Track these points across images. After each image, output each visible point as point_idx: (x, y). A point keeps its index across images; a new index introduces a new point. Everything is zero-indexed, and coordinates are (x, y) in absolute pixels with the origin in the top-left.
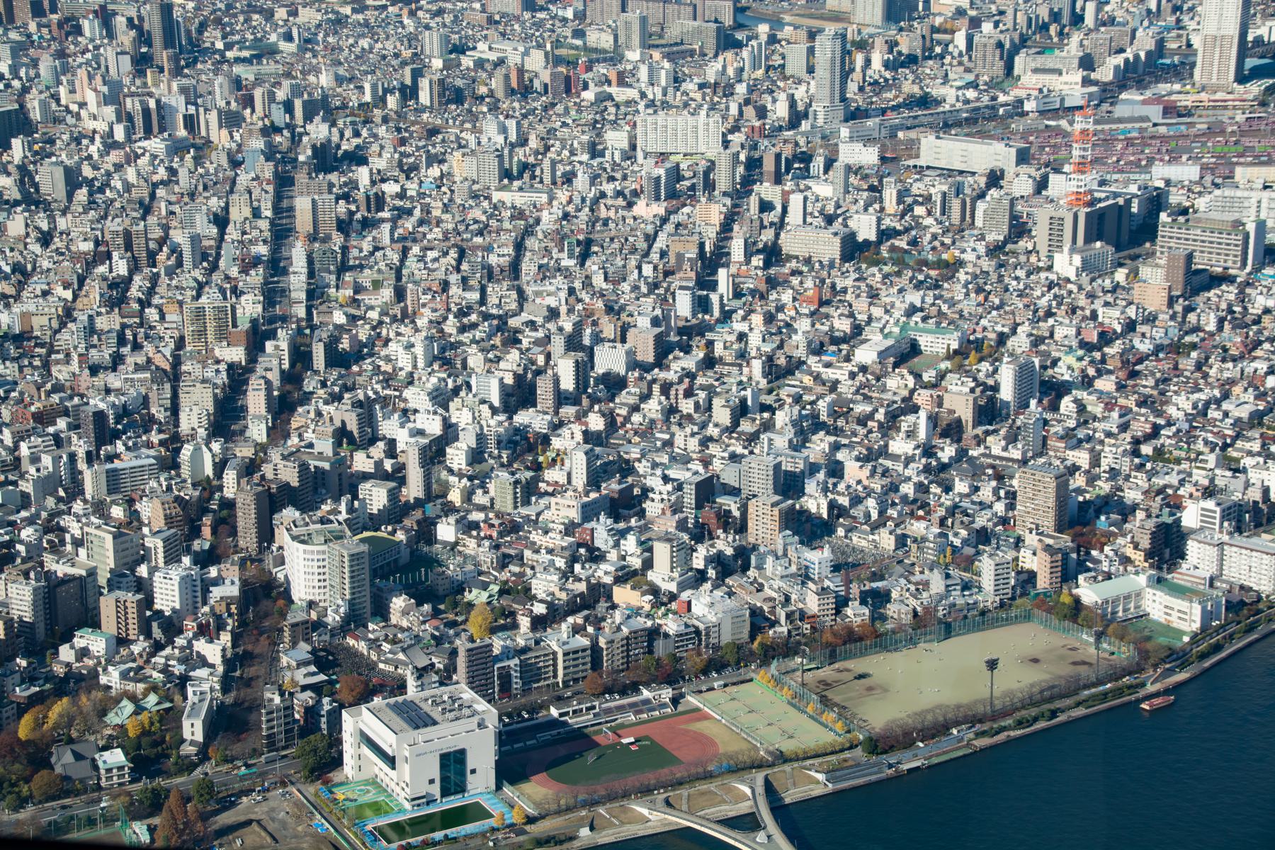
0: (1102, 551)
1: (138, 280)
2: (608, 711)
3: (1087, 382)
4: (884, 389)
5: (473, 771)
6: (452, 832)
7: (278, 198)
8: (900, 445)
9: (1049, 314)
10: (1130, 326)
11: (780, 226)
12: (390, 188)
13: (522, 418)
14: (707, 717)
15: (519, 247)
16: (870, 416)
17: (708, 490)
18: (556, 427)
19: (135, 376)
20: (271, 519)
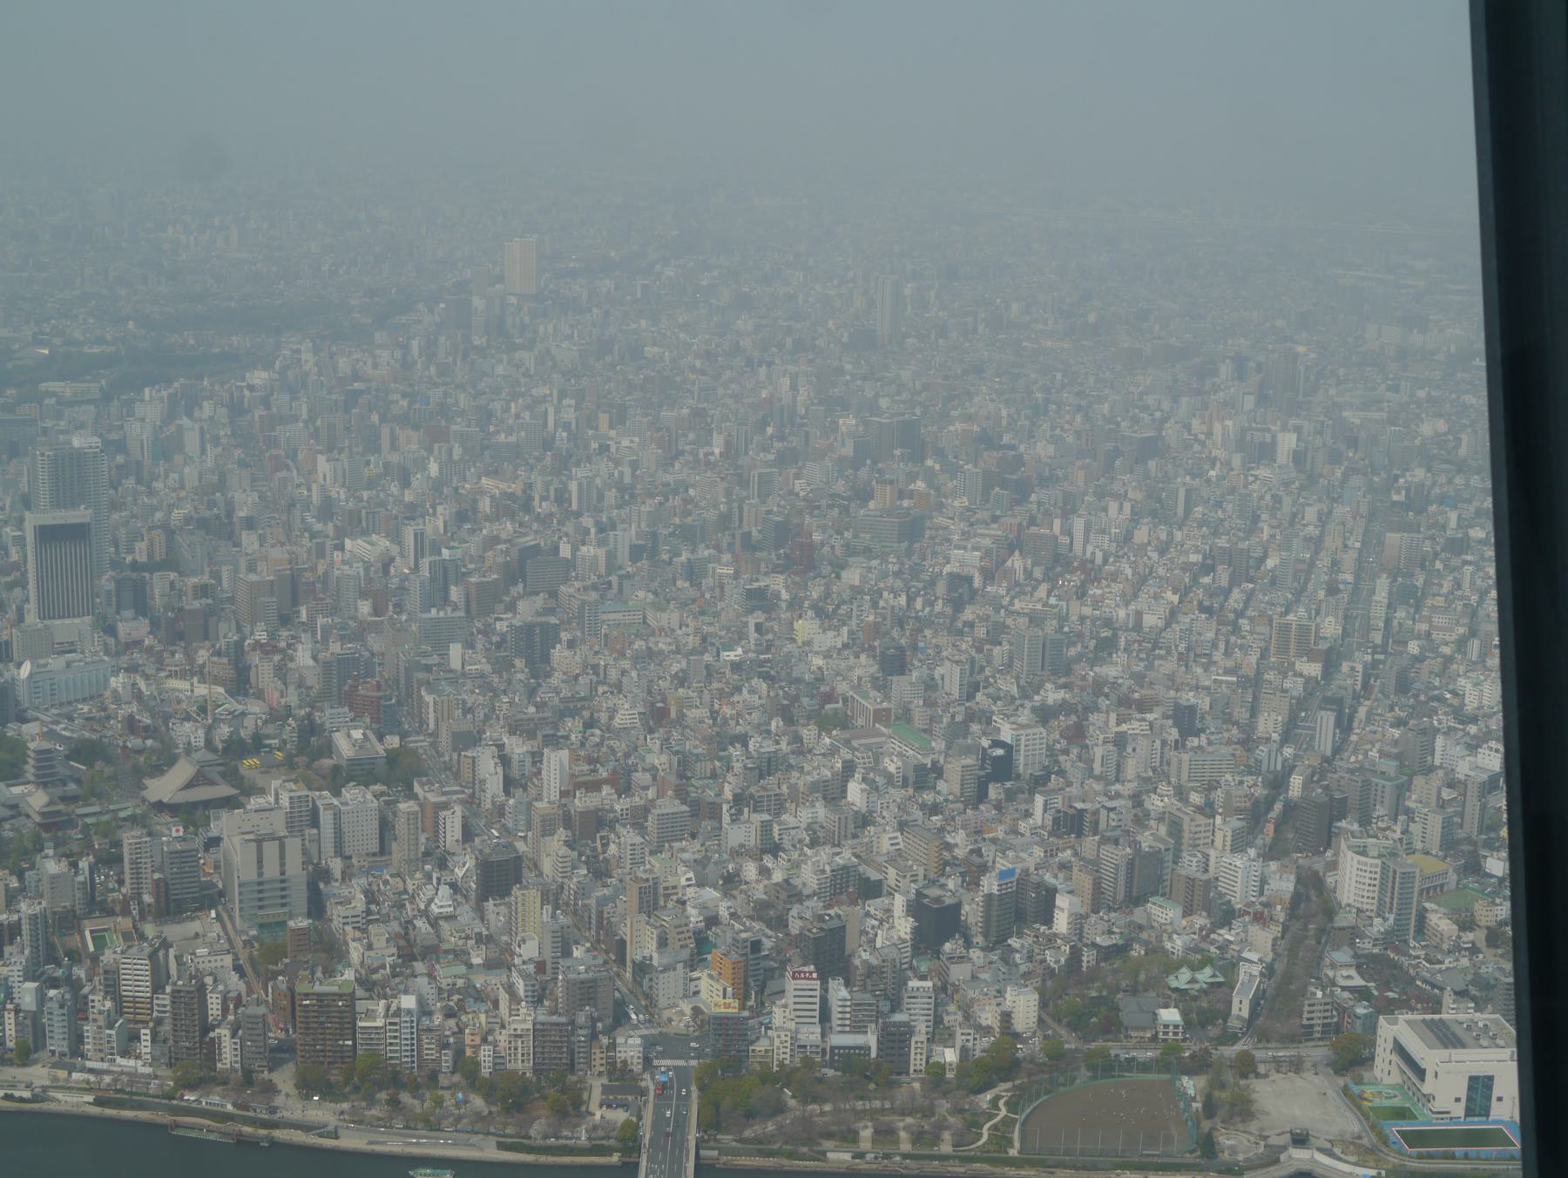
1: (1236, 591)
5: (1500, 1099)
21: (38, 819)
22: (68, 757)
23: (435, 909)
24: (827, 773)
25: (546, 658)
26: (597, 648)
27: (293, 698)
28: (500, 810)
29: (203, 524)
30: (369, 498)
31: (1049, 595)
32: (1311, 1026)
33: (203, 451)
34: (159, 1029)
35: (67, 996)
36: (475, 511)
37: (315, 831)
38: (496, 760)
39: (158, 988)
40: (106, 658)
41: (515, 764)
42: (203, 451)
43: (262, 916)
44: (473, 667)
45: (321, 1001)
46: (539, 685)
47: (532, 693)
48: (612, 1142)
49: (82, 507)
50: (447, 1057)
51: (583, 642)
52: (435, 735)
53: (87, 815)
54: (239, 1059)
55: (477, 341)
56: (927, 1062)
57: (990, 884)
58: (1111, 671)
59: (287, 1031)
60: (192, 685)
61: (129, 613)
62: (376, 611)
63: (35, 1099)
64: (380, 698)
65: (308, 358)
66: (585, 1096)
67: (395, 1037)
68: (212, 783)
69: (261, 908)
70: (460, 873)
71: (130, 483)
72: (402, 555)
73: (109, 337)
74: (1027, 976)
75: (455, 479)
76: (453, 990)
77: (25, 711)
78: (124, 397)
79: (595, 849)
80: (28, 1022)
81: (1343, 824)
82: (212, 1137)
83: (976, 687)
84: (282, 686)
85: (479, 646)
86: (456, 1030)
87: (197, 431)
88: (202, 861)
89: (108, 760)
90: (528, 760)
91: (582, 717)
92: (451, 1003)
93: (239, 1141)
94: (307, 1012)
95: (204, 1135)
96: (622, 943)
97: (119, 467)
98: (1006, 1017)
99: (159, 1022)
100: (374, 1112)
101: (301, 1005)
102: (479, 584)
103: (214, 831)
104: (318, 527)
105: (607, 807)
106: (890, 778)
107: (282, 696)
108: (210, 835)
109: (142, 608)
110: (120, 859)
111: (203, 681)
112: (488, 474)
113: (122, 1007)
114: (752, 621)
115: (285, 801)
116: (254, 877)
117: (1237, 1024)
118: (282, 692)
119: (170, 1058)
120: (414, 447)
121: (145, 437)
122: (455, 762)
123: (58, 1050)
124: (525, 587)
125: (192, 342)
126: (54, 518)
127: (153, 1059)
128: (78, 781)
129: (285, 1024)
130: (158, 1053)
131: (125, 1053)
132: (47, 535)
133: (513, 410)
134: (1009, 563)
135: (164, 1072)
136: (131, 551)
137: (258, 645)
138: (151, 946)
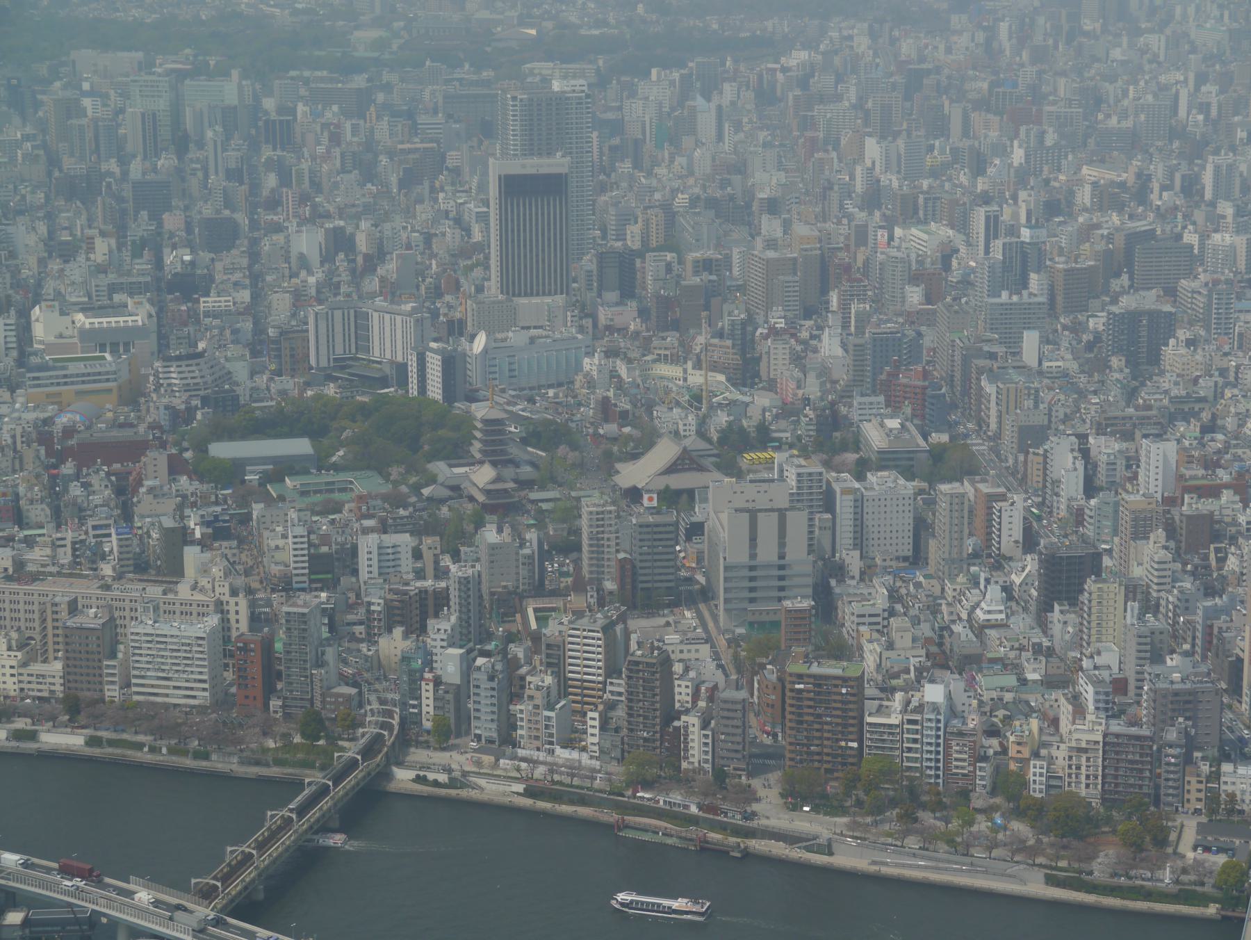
21: (481, 498)
22: (525, 441)
23: (980, 615)
25: (1155, 358)
26: (1227, 348)
27: (812, 388)
28: (1078, 517)
29: (712, 203)
30: (930, 187)
33: (720, 138)
34: (612, 714)
35: (499, 667)
36: (1070, 204)
37: (829, 516)
38: (1076, 454)
39: (612, 671)
40: (580, 336)
41: (1102, 469)
42: (720, 138)
43: (754, 612)
44: (1054, 364)
45: (820, 686)
46: (1143, 384)
47: (1131, 395)
48: (1207, 889)
49: (559, 154)
50: (984, 773)
51: (1207, 341)
52: (998, 436)
53: (542, 501)
54: (710, 757)
55: (1088, 25)
59: (775, 736)
60: (685, 371)
61: (612, 296)
62: (929, 299)
63: (453, 784)
64: (925, 388)
65: (862, 43)
66: (1173, 836)
67: (915, 741)
68: (701, 469)
69: (752, 600)
70: (1017, 579)
71: (625, 166)
72: (968, 244)
73: (612, 21)
75: (1046, 168)
76: (998, 703)
77: (477, 390)
78: (623, 79)
79: (1206, 558)
80: (450, 697)
82: (669, 841)
84: (797, 373)
85: (1065, 344)
86: (999, 749)
87: (713, 113)
88: (682, 555)
89: (574, 447)
90: (1121, 463)
91: (1199, 420)
92: (995, 720)
93: (703, 849)
94: (799, 699)
95: (659, 838)
96: (1240, 661)
97: (613, 149)
99: (611, 706)
100: (887, 827)
101: (792, 690)
102: (1068, 272)
103: (698, 516)
104: (861, 216)
105: (1227, 519)
107: (799, 387)
108: (694, 519)
109: (628, 287)
110: (578, 548)
111: (698, 365)
112: (1090, 163)
113: (566, 686)
116: (744, 559)
118: (799, 381)
119: (623, 751)
120: (994, 134)
121: (647, 119)
122: (1021, 468)
123: (485, 734)
124: (1131, 278)
125: (715, 26)
126: (524, 166)
127: (601, 751)
128: (533, 465)
129: (773, 727)
130: (607, 745)
131: (568, 744)
132: (513, 187)
133: (1131, 95)
135: (614, 767)
136: (621, 237)
137: (774, 332)
138: (606, 617)
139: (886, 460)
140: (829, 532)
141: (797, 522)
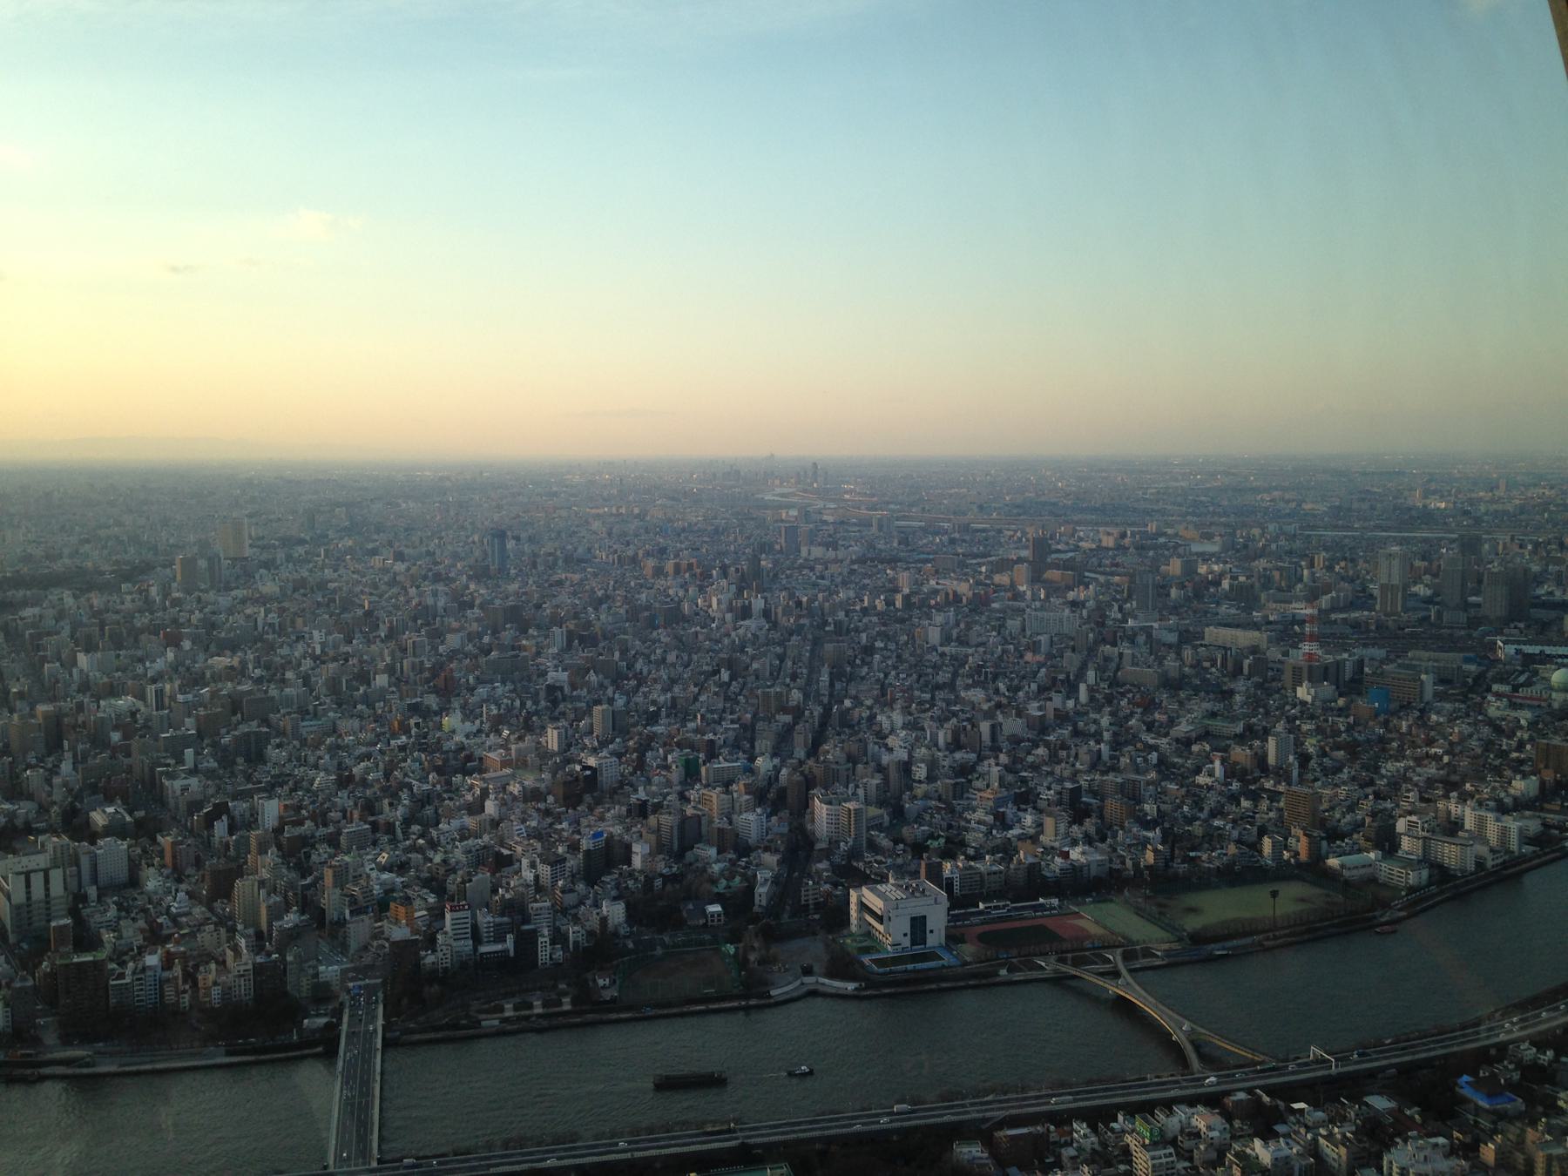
0: (1343, 841)
2: (1016, 909)
3: (1324, 754)
4: (1191, 753)
6: (919, 966)
7: (810, 673)
8: (1202, 779)
9: (1296, 718)
10: (1350, 728)
11: (1118, 668)
12: (879, 644)
13: (958, 755)
14: (1083, 917)
15: (955, 675)
16: (1183, 766)
17: (1076, 793)
18: (981, 759)
19: (732, 726)
20: (807, 794)
24: (469, 797)
31: (614, 693)
32: (808, 905)
56: (551, 957)
57: (586, 844)
58: (659, 729)
62: (126, 737)
74: (615, 899)
81: (815, 791)
83: (569, 745)
98: (604, 920)
106: (515, 798)
114: (412, 722)
115: (50, 847)
117: (760, 910)
134: (587, 678)
139: (109, 831)
140: (76, 878)
141: (56, 876)
